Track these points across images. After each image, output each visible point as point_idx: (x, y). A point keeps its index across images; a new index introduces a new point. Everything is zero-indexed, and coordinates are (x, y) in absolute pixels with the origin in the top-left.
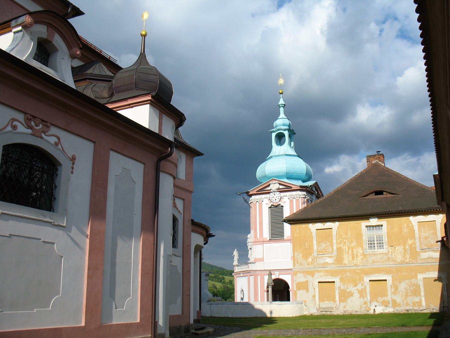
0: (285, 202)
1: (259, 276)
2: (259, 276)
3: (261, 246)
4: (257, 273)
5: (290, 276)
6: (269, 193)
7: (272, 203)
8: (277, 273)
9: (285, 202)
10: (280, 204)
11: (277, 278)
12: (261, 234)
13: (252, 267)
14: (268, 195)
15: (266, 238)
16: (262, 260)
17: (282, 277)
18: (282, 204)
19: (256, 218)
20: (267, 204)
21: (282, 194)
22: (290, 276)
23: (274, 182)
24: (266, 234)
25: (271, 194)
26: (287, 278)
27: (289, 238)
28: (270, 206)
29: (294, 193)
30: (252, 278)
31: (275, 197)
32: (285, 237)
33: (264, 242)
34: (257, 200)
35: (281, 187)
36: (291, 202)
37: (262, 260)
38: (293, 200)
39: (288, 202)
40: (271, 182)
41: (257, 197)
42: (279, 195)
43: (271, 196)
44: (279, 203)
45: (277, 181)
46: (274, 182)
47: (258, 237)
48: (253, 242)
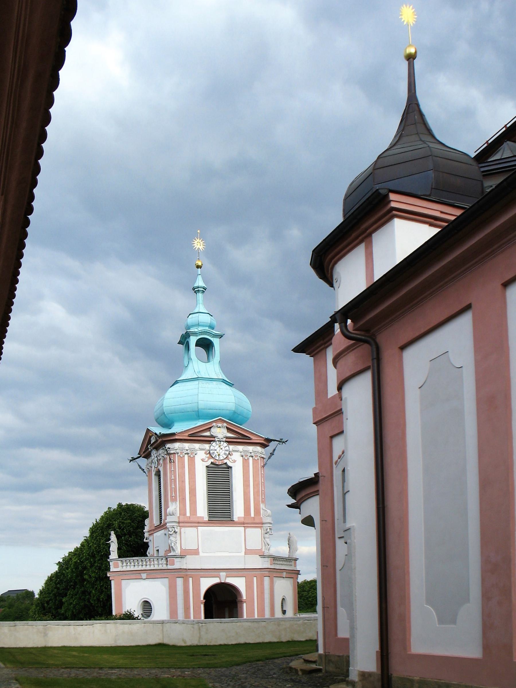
0: (235, 461)
1: (191, 579)
2: (191, 579)
3: (195, 529)
4: (189, 573)
5: (243, 580)
6: (209, 442)
7: (212, 460)
8: (223, 574)
9: (235, 461)
10: (226, 463)
11: (223, 582)
12: (194, 510)
13: (178, 564)
14: (207, 446)
15: (203, 517)
16: (196, 552)
17: (230, 581)
18: (230, 464)
19: (183, 482)
20: (203, 460)
21: (232, 447)
22: (243, 580)
23: (220, 425)
24: (202, 511)
25: (214, 444)
26: (240, 583)
27: (242, 520)
28: (209, 463)
29: (251, 448)
30: (180, 582)
31: (220, 450)
32: (235, 519)
33: (199, 523)
34: (186, 452)
35: (230, 435)
36: (245, 463)
37: (196, 552)
38: (248, 459)
39: (240, 460)
40: (214, 424)
41: (186, 445)
42: (227, 448)
43: (212, 448)
44: (225, 461)
45: (225, 424)
46: (220, 425)
47: (188, 514)
48: (179, 523)
